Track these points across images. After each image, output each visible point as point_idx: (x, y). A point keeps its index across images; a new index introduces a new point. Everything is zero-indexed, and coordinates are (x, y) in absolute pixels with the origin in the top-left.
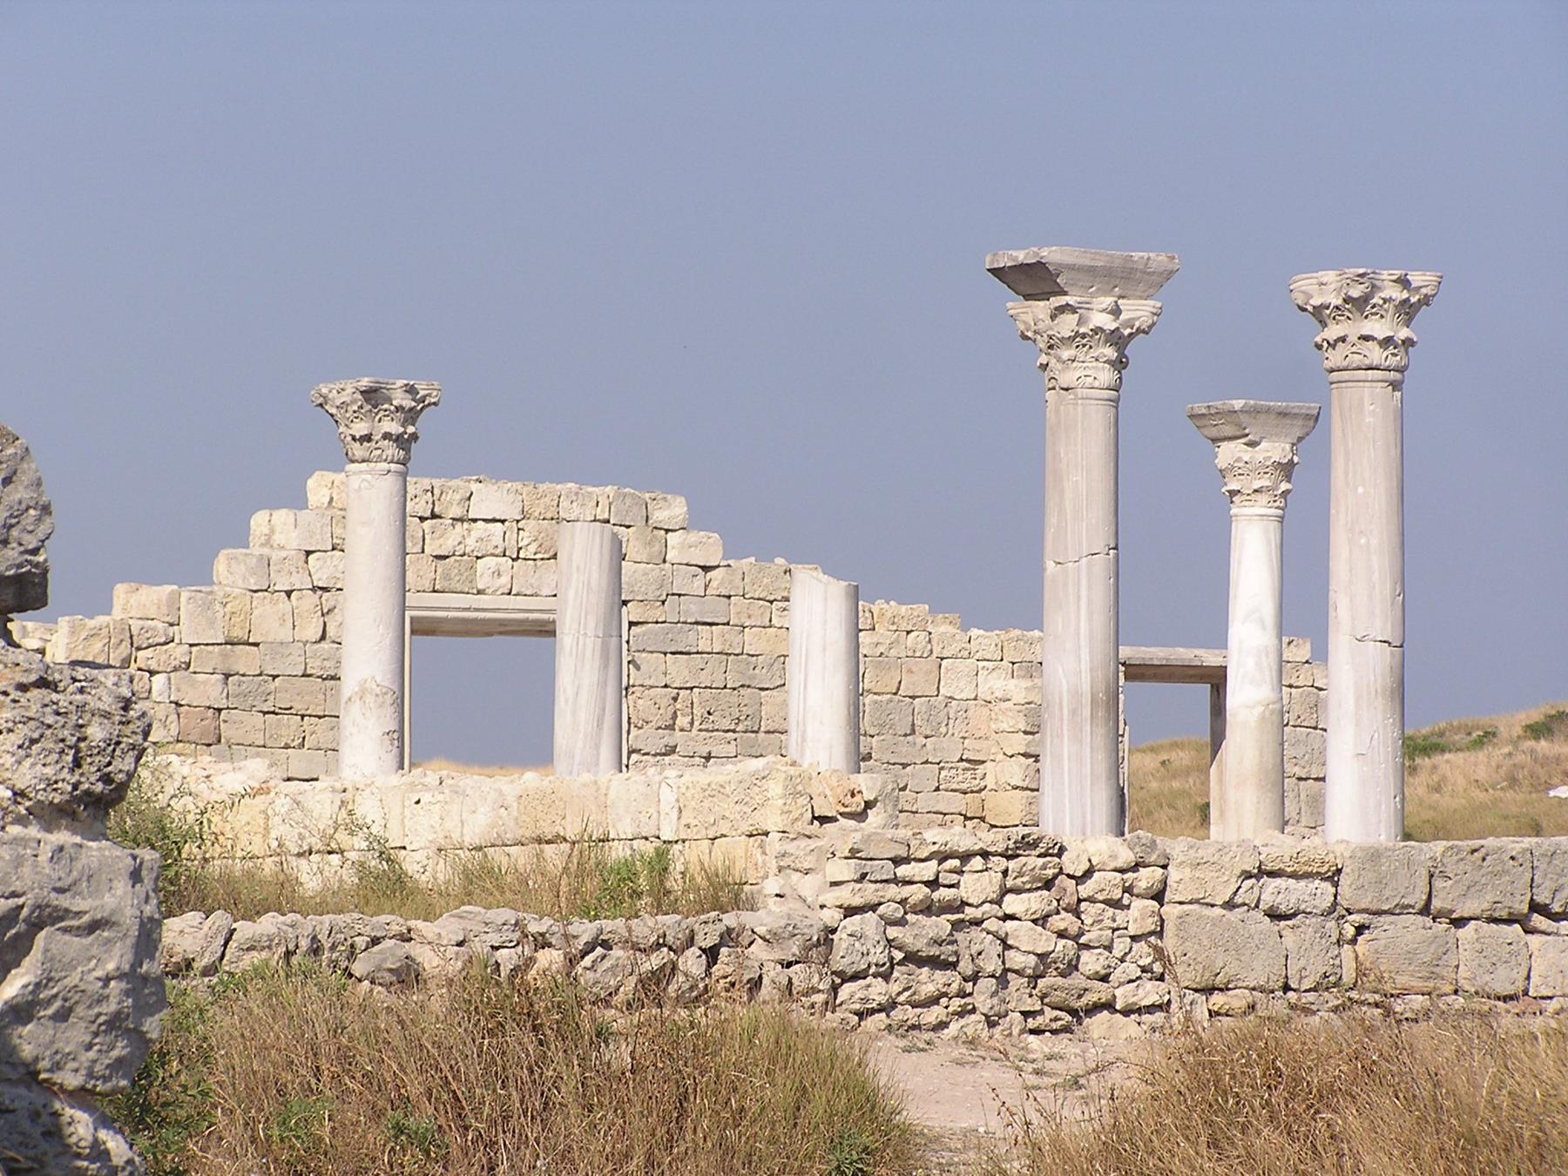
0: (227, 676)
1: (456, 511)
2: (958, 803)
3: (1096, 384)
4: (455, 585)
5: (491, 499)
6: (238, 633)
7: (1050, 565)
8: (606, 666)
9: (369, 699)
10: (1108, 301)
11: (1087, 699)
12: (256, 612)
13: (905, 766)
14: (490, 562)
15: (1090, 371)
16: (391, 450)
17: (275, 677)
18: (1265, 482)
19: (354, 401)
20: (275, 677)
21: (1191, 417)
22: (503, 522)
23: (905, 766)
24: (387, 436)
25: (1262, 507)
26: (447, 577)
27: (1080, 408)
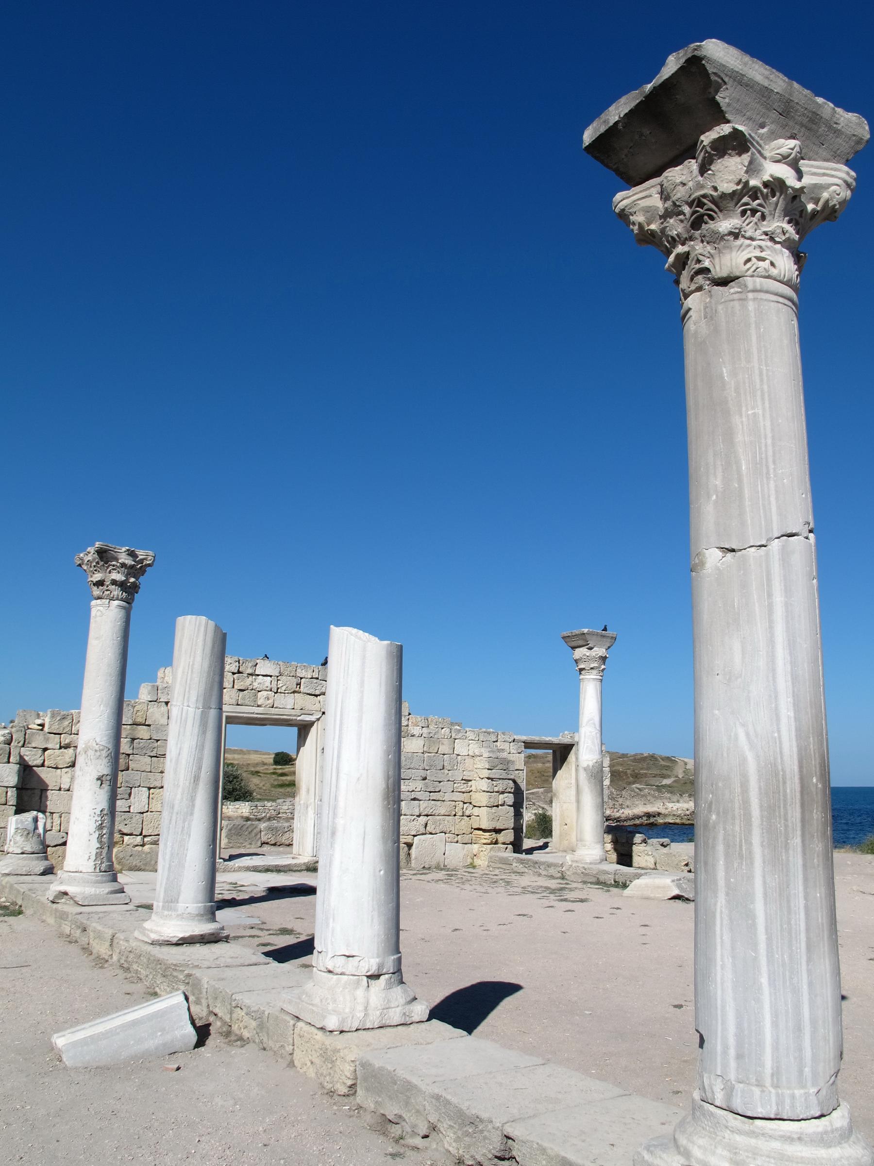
0: (133, 739)
1: (250, 671)
2: (462, 797)
3: (774, 272)
4: (247, 702)
5: (264, 667)
6: (139, 720)
7: (713, 557)
8: (204, 732)
9: (91, 753)
10: (788, 145)
11: (793, 786)
12: (150, 711)
13: (440, 782)
14: (264, 693)
15: (759, 257)
16: (116, 591)
17: (158, 741)
18: (595, 665)
19: (94, 559)
20: (158, 741)
21: (563, 638)
22: (271, 676)
23: (440, 782)
24: (114, 582)
25: (593, 675)
26: (244, 699)
27: (751, 306)
